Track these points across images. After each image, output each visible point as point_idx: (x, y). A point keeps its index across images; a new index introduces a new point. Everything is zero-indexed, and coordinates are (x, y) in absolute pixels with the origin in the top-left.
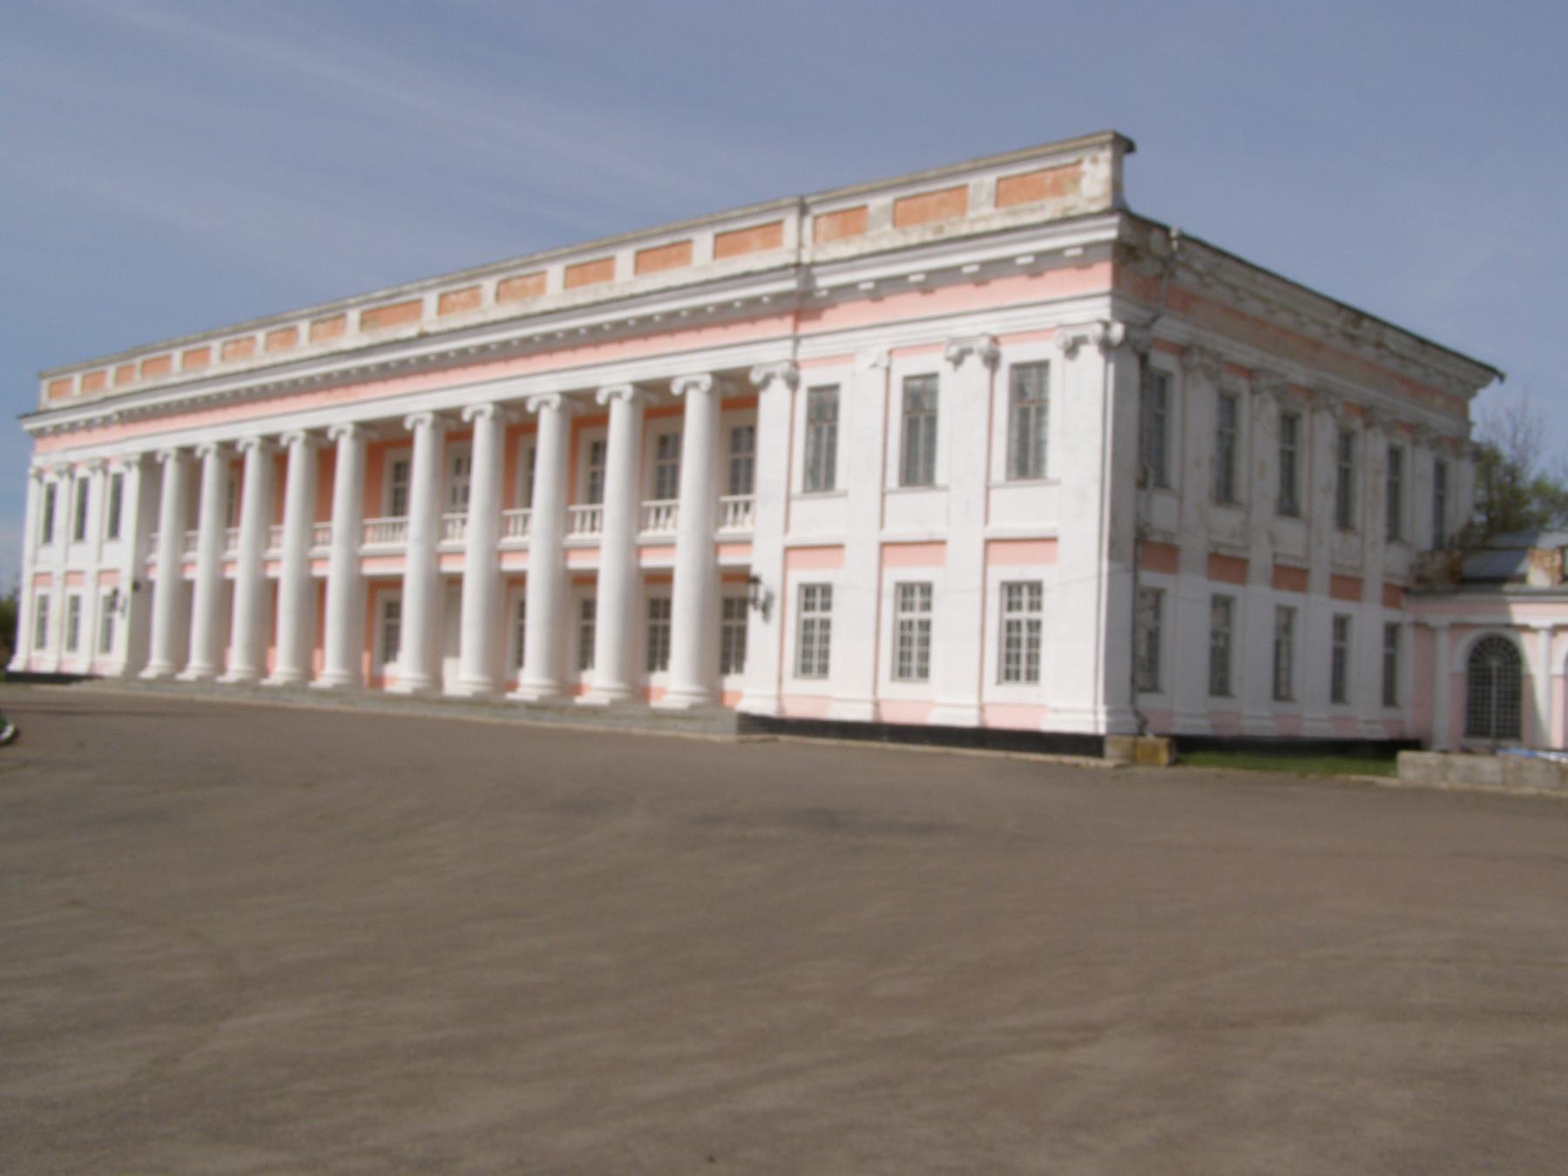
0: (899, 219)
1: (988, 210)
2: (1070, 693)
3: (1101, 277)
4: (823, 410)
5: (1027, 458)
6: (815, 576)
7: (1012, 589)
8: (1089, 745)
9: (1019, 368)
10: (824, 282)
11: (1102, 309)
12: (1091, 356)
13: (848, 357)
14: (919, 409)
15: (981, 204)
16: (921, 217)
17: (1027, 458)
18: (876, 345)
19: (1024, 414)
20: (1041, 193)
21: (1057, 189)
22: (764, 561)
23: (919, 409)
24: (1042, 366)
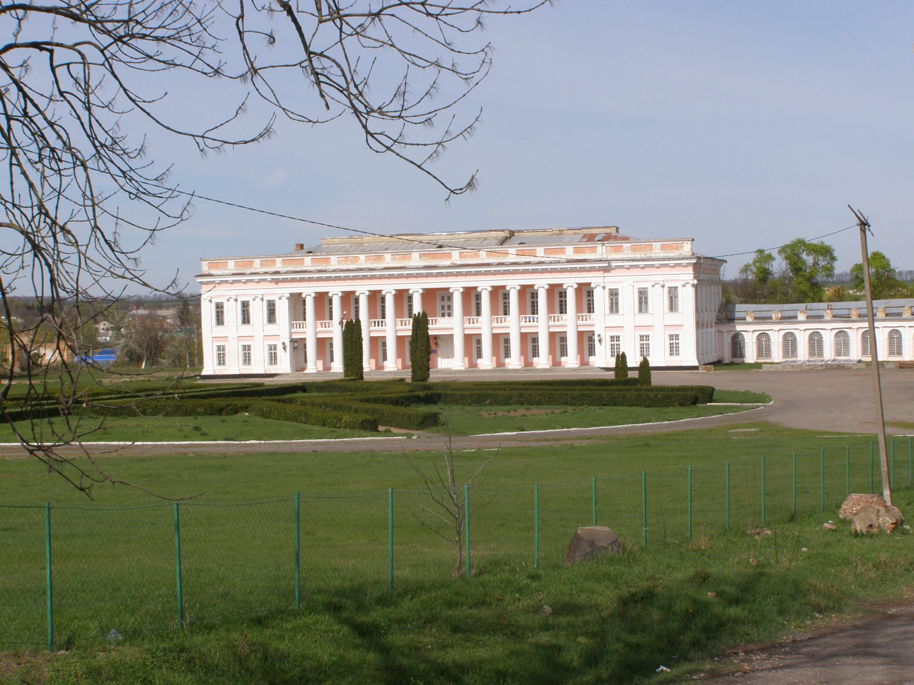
0: (634, 250)
1: (659, 251)
2: (688, 356)
3: (690, 270)
4: (614, 294)
5: (673, 307)
6: (615, 333)
7: (671, 336)
8: (696, 368)
9: (670, 288)
10: (613, 264)
11: (692, 276)
12: (689, 287)
13: (621, 282)
14: (643, 296)
15: (657, 250)
16: (640, 250)
17: (673, 307)
18: (630, 280)
19: (671, 298)
20: (673, 249)
21: (677, 248)
22: (598, 330)
23: (643, 296)
24: (676, 288)
